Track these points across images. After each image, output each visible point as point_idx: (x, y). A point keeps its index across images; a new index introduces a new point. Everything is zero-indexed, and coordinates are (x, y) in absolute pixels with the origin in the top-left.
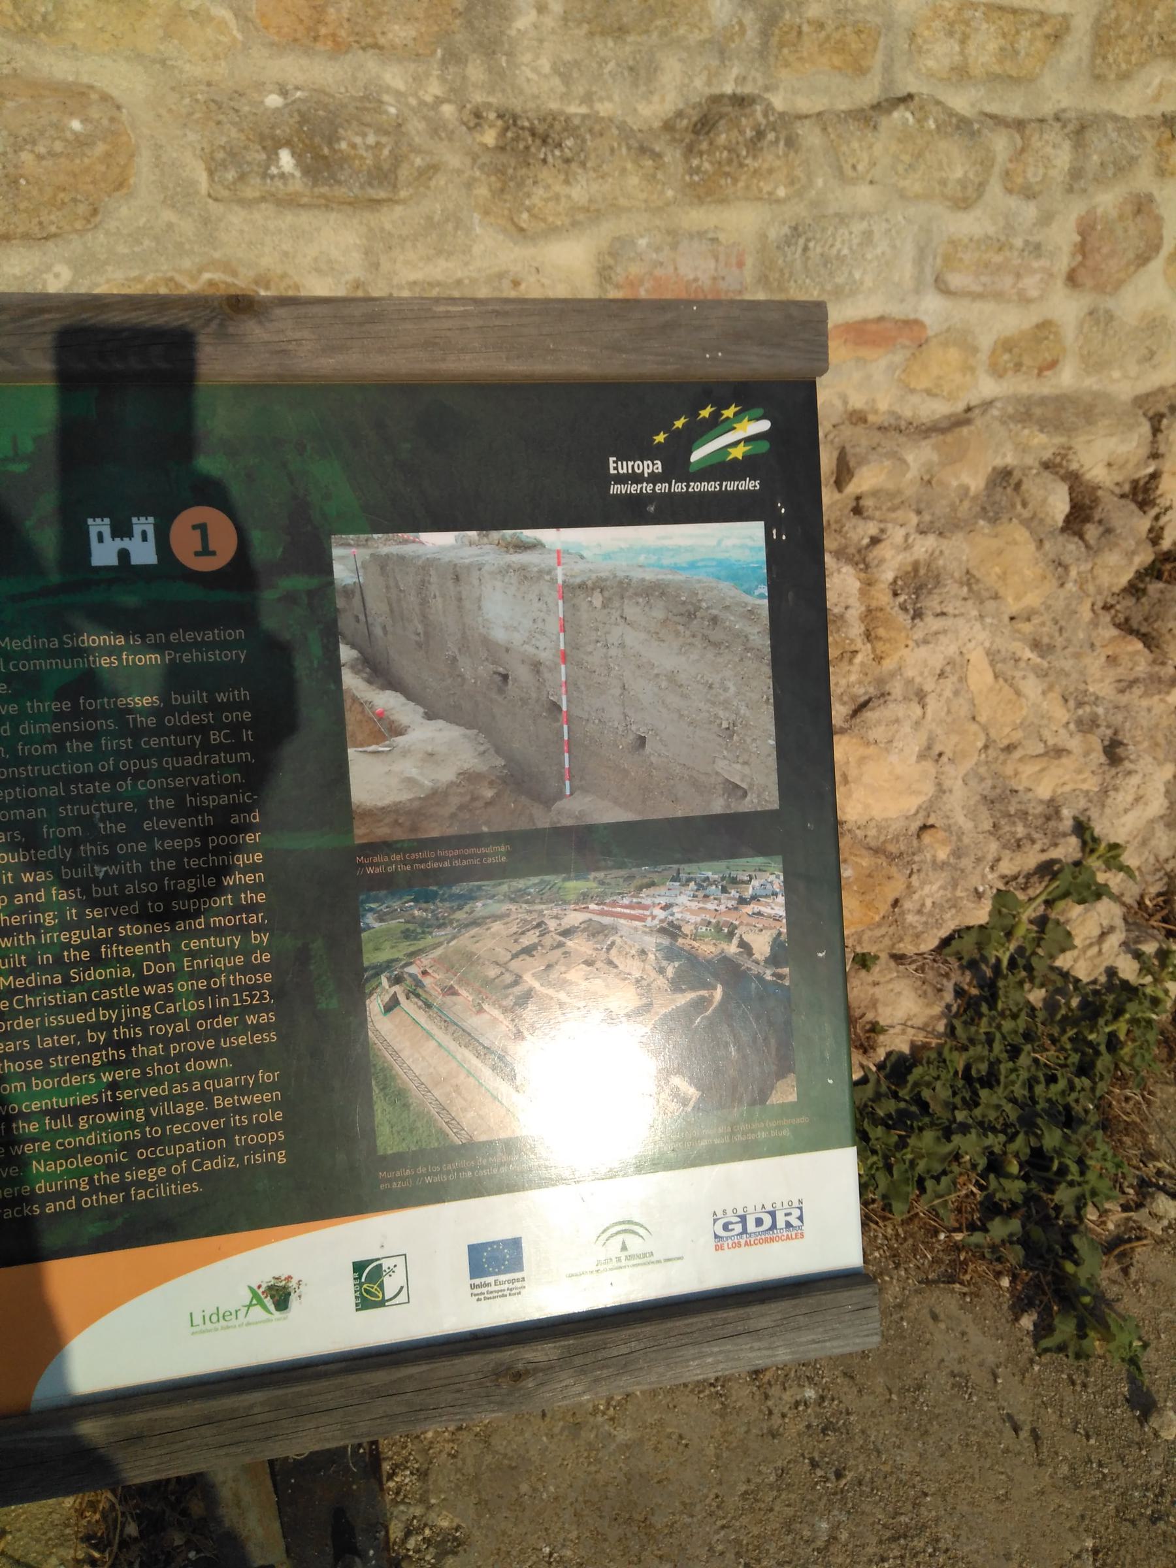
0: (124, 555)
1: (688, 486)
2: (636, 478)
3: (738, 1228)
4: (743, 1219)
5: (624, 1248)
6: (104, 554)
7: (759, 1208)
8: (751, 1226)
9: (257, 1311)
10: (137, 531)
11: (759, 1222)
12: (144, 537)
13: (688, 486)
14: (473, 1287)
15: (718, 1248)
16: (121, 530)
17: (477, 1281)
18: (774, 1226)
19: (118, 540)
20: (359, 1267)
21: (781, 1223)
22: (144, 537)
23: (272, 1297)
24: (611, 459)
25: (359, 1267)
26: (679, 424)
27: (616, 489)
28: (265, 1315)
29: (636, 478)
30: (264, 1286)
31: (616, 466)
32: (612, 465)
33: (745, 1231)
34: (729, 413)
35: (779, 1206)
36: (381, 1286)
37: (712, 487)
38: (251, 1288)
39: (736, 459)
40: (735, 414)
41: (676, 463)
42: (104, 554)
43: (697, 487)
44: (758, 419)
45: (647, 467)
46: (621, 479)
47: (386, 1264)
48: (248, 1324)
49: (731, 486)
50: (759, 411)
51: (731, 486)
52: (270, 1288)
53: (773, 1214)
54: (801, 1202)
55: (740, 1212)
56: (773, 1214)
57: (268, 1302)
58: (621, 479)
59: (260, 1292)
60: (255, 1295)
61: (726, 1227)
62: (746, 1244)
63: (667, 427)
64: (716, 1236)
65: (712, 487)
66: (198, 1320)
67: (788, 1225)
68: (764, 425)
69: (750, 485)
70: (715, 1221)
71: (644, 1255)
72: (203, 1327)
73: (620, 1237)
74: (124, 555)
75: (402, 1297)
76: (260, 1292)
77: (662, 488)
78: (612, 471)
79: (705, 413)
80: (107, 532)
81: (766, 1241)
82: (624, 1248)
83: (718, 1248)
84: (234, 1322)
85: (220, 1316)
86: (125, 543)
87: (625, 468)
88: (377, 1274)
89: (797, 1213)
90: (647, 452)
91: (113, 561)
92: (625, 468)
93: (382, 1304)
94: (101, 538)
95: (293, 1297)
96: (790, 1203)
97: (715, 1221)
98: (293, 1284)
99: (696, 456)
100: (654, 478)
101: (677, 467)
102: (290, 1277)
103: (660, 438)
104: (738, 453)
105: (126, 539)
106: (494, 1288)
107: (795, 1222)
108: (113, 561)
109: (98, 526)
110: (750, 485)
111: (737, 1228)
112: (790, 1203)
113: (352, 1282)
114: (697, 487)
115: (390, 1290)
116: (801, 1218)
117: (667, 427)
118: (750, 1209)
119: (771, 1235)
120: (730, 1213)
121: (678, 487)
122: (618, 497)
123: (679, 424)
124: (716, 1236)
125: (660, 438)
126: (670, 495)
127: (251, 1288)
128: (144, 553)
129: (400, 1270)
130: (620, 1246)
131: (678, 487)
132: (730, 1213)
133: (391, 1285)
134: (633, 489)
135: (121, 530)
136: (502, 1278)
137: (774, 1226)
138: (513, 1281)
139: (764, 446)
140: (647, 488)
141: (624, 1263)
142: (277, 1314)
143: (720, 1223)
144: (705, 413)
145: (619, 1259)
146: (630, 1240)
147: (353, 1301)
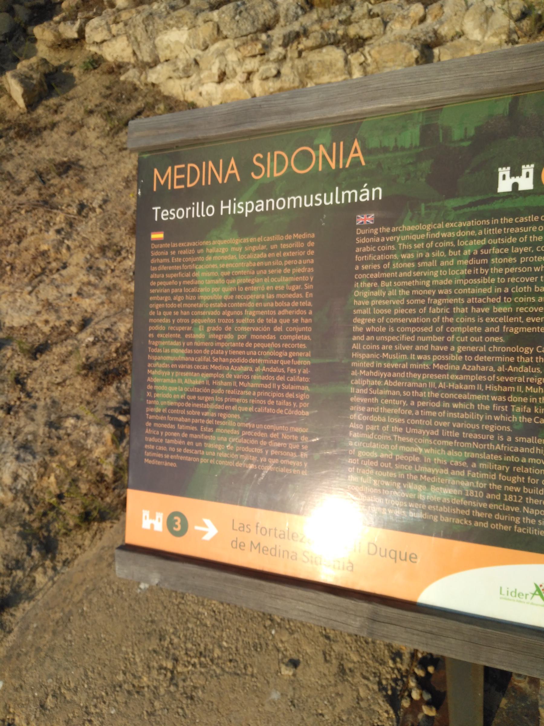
0: (515, 185)
6: (504, 186)
12: (528, 175)
16: (516, 172)
19: (513, 178)
22: (528, 175)
38: (536, 586)
42: (504, 186)
48: (532, 604)
74: (515, 185)
76: (541, 588)
80: (508, 174)
86: (517, 179)
94: (504, 177)
108: (509, 189)
109: (504, 171)
127: (536, 586)
128: (526, 183)
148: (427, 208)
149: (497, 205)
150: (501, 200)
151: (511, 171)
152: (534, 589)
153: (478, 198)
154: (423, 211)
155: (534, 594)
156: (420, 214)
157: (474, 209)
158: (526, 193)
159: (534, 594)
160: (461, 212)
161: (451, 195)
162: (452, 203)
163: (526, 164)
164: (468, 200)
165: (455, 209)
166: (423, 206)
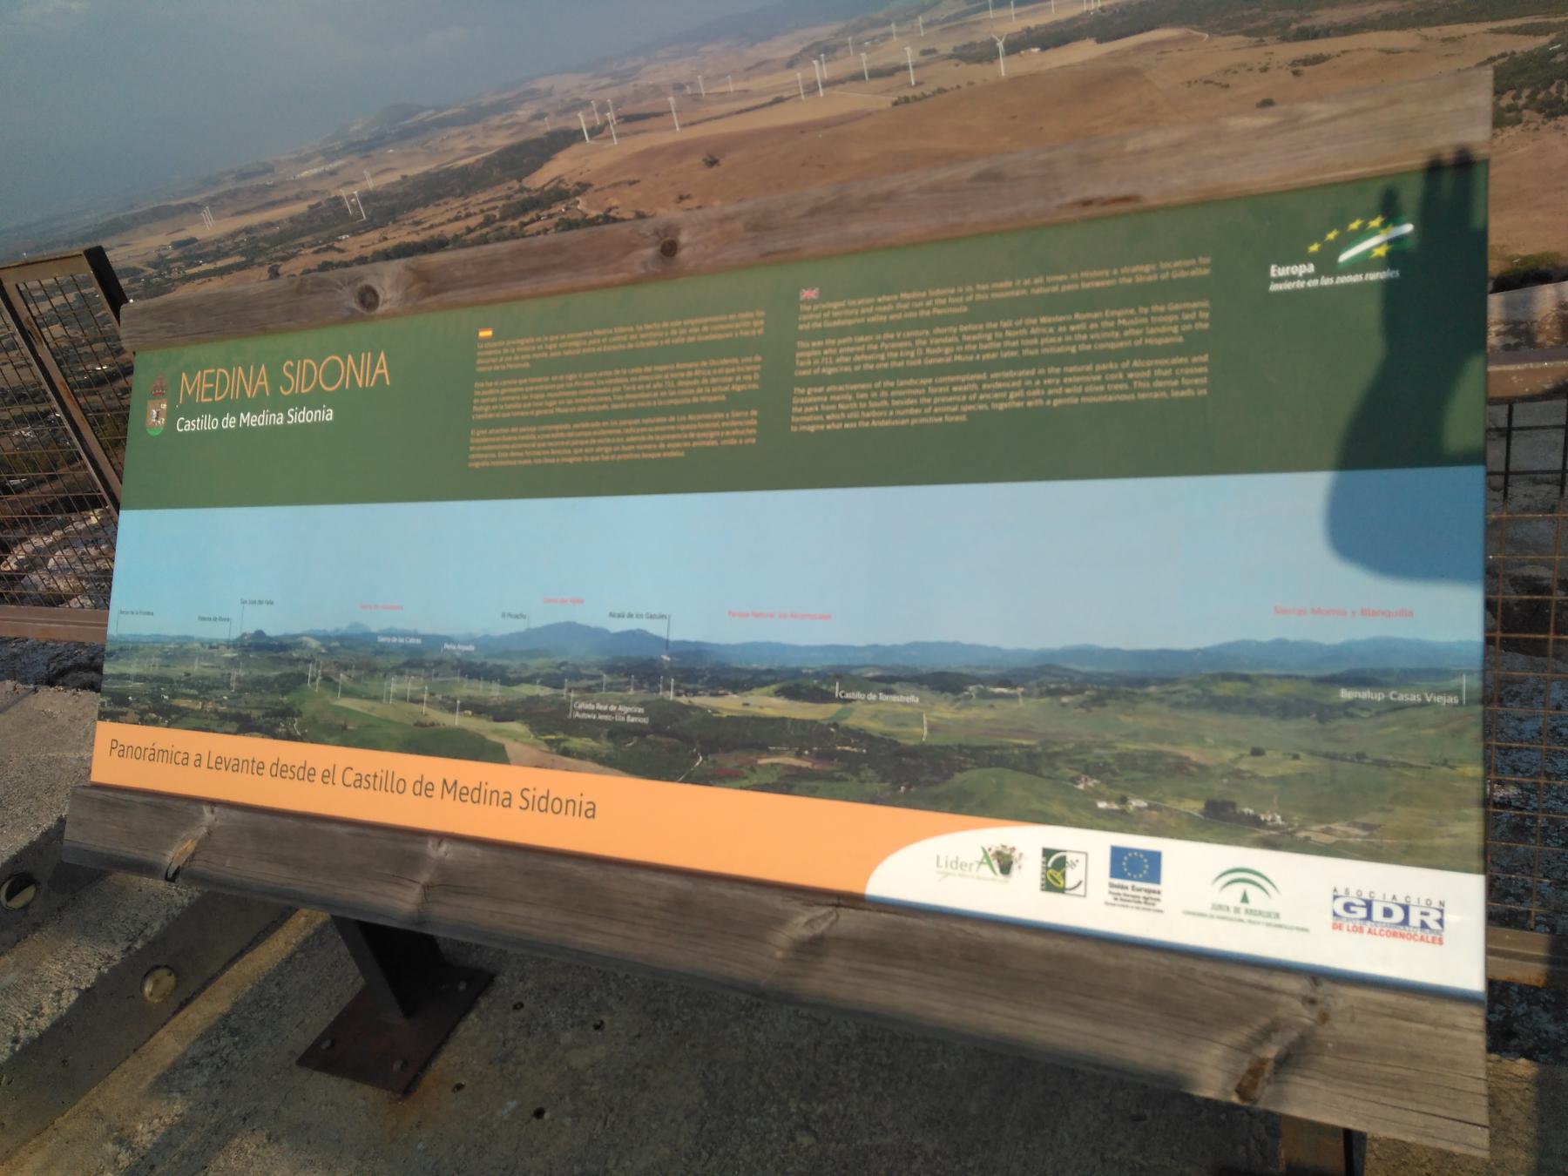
3: (1362, 913)
4: (1369, 905)
5: (1245, 899)
7: (1389, 898)
9: (986, 869)
11: (1388, 913)
18: (1405, 922)
21: (1415, 919)
28: (990, 874)
36: (1064, 875)
41: (1326, 264)
45: (1300, 270)
53: (1406, 909)
54: (1442, 904)
55: (1366, 896)
56: (1406, 909)
57: (995, 863)
61: (1347, 907)
62: (1370, 931)
63: (1320, 238)
64: (1335, 914)
67: (1424, 925)
70: (1335, 897)
73: (1238, 889)
77: (1313, 283)
81: (1394, 935)
82: (1245, 899)
89: (1437, 915)
90: (1303, 258)
97: (1335, 897)
100: (1306, 277)
101: (1326, 264)
103: (1314, 248)
107: (1431, 921)
112: (1429, 903)
115: (1070, 881)
116: (1441, 922)
117: (1320, 238)
118: (1378, 896)
119: (1401, 929)
120: (1353, 893)
124: (1335, 914)
125: (1314, 248)
130: (1240, 896)
132: (1353, 893)
137: (1405, 922)
140: (1300, 284)
141: (1242, 915)
142: (1001, 877)
145: (1237, 910)
146: (1251, 889)
152: (981, 854)
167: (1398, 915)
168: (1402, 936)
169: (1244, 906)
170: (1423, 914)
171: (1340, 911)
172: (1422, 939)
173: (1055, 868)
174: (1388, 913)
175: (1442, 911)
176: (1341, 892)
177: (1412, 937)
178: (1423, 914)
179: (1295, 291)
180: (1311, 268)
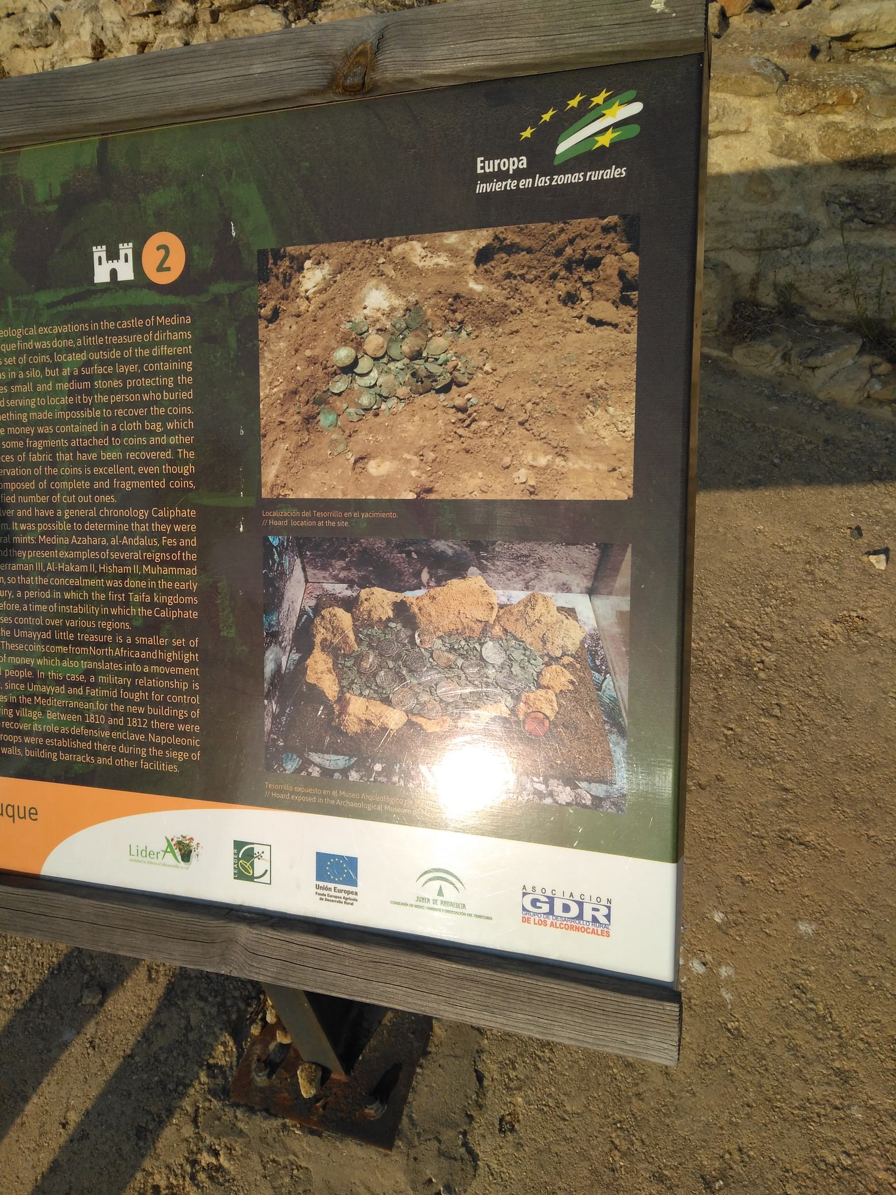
0: (114, 273)
1: (551, 180)
2: (502, 175)
3: (546, 908)
4: (551, 901)
5: (440, 893)
7: (567, 896)
8: (558, 910)
9: (169, 856)
10: (122, 254)
11: (566, 908)
13: (551, 180)
14: (318, 887)
15: (525, 920)
17: (321, 884)
18: (580, 917)
19: (110, 262)
20: (238, 845)
21: (588, 915)
23: (180, 850)
24: (479, 159)
25: (238, 845)
26: (546, 117)
27: (482, 188)
29: (502, 175)
30: (175, 840)
31: (483, 166)
32: (479, 165)
33: (551, 912)
34: (599, 100)
35: (587, 899)
36: (252, 865)
37: (576, 178)
39: (603, 147)
40: (605, 100)
41: (541, 158)
42: (101, 275)
43: (560, 179)
44: (629, 102)
45: (513, 164)
46: (487, 178)
47: (257, 849)
48: (164, 865)
49: (595, 176)
50: (632, 94)
51: (595, 176)
52: (179, 843)
53: (580, 904)
54: (609, 901)
55: (549, 894)
56: (580, 904)
57: (177, 852)
58: (487, 178)
59: (173, 843)
60: (169, 845)
61: (534, 902)
62: (552, 925)
63: (534, 120)
64: (524, 909)
65: (576, 178)
66: (134, 852)
67: (595, 920)
68: (637, 108)
69: (616, 172)
70: (524, 894)
71: (458, 906)
72: (137, 858)
73: (436, 884)
74: (114, 273)
75: (266, 879)
78: (479, 171)
79: (574, 103)
80: (104, 255)
81: (572, 928)
82: (440, 893)
83: (525, 920)
84: (153, 861)
85: (147, 853)
86: (114, 265)
87: (491, 166)
88: (250, 855)
89: (606, 911)
91: (107, 279)
92: (491, 166)
93: (251, 879)
95: (193, 854)
96: (599, 899)
97: (524, 894)
98: (194, 844)
99: (562, 148)
100: (519, 174)
101: (541, 158)
102: (192, 839)
103: (527, 134)
104: (605, 141)
105: (115, 261)
106: (332, 893)
108: (107, 279)
109: (99, 252)
110: (616, 172)
111: (542, 906)
113: (232, 856)
114: (560, 179)
116: (608, 917)
117: (534, 120)
118: (559, 894)
119: (576, 923)
120: (538, 891)
121: (542, 181)
122: (486, 195)
123: (546, 117)
124: (524, 909)
125: (527, 134)
126: (534, 190)
128: (126, 272)
129: (266, 856)
131: (542, 181)
132: (538, 891)
133: (259, 867)
134: (498, 186)
135: (113, 255)
136: (340, 887)
137: (580, 917)
138: (349, 892)
139: (634, 130)
140: (511, 184)
141: (439, 906)
143: (529, 898)
144: (574, 103)
145: (435, 901)
147: (232, 871)
148: (15, 303)
149: (95, 303)
150: (99, 295)
151: (107, 251)
153: (73, 291)
154: (11, 309)
155: (166, 852)
156: (7, 313)
157: (69, 307)
158: (126, 285)
159: (166, 852)
160: (54, 311)
161: (41, 287)
162: (44, 297)
163: (123, 243)
164: (62, 294)
165: (50, 306)
166: (10, 299)
167: (575, 911)
168: (578, 929)
169: (440, 898)
170: (594, 909)
171: (529, 907)
172: (593, 932)
173: (245, 857)
174: (566, 908)
175: (609, 908)
176: (529, 890)
177: (586, 930)
178: (594, 909)
179: (506, 192)
180: (524, 163)
